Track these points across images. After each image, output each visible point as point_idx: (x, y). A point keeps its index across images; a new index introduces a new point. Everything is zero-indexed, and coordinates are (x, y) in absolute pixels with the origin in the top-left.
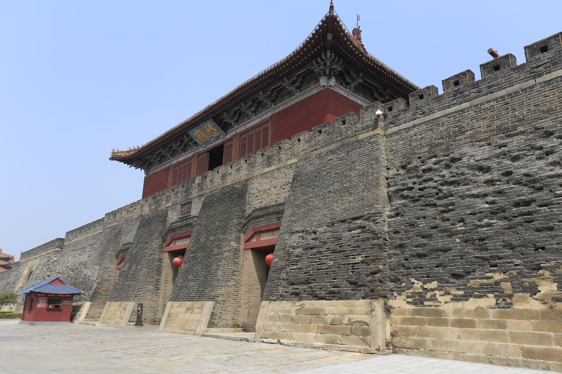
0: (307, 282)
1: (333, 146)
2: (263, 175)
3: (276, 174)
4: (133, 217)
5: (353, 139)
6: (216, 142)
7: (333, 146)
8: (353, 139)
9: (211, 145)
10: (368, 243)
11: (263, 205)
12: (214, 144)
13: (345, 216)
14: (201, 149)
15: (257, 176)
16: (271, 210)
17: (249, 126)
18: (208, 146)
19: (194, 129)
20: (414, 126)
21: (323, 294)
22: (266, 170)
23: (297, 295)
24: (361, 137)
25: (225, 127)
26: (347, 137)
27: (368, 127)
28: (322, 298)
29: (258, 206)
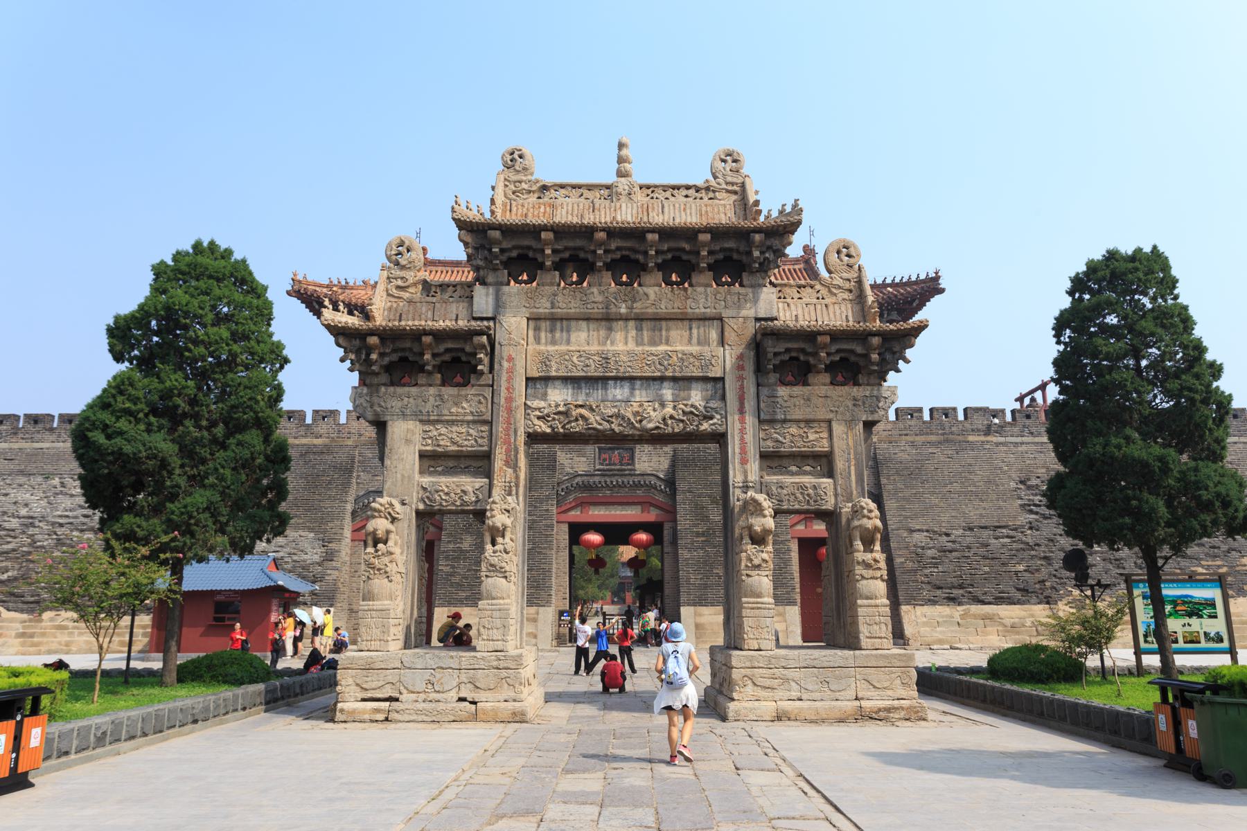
0: (961, 587)
1: (933, 438)
5: (960, 438)
7: (933, 438)
8: (960, 438)
10: (1026, 554)
13: (983, 522)
20: (1022, 443)
21: (990, 599)
23: (952, 600)
24: (971, 438)
26: (952, 433)
27: (979, 430)
28: (990, 603)
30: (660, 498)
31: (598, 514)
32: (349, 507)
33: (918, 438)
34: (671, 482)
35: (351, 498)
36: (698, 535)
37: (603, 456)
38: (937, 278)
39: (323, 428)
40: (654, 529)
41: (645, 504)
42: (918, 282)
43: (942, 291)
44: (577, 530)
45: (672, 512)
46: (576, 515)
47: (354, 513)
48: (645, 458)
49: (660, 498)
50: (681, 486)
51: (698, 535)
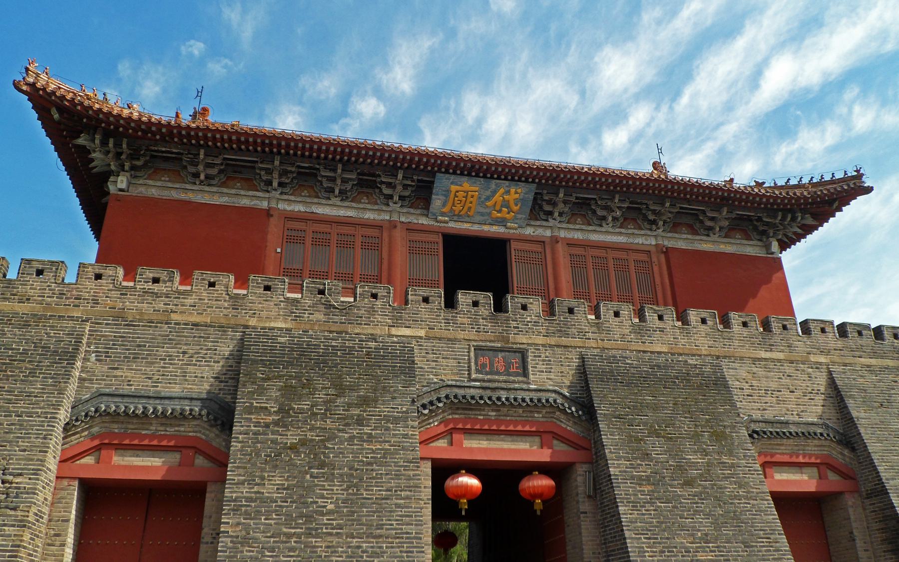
2: (755, 360)
3: (788, 369)
4: (175, 317)
6: (486, 228)
9: (466, 226)
11: (769, 415)
12: (476, 227)
14: (423, 221)
15: (742, 358)
16: (793, 429)
17: (594, 237)
18: (451, 224)
19: (466, 178)
22: (764, 355)
25: (538, 210)
29: (757, 415)
30: (568, 426)
31: (478, 447)
32: (63, 415)
33: (873, 361)
34: (584, 405)
35: (67, 404)
36: (640, 481)
37: (481, 360)
38: (859, 176)
39: (34, 286)
40: (557, 471)
41: (545, 435)
42: (832, 182)
43: (869, 190)
44: (443, 471)
45: (591, 449)
46: (442, 448)
47: (67, 428)
48: (541, 367)
49: (568, 426)
50: (602, 410)
51: (640, 481)
